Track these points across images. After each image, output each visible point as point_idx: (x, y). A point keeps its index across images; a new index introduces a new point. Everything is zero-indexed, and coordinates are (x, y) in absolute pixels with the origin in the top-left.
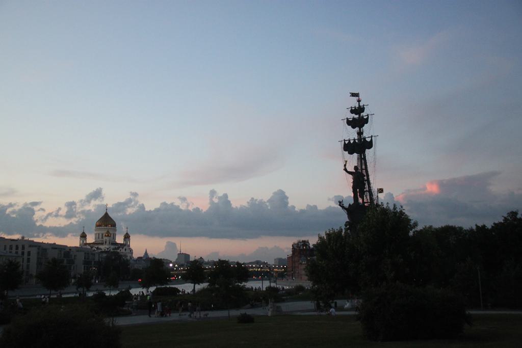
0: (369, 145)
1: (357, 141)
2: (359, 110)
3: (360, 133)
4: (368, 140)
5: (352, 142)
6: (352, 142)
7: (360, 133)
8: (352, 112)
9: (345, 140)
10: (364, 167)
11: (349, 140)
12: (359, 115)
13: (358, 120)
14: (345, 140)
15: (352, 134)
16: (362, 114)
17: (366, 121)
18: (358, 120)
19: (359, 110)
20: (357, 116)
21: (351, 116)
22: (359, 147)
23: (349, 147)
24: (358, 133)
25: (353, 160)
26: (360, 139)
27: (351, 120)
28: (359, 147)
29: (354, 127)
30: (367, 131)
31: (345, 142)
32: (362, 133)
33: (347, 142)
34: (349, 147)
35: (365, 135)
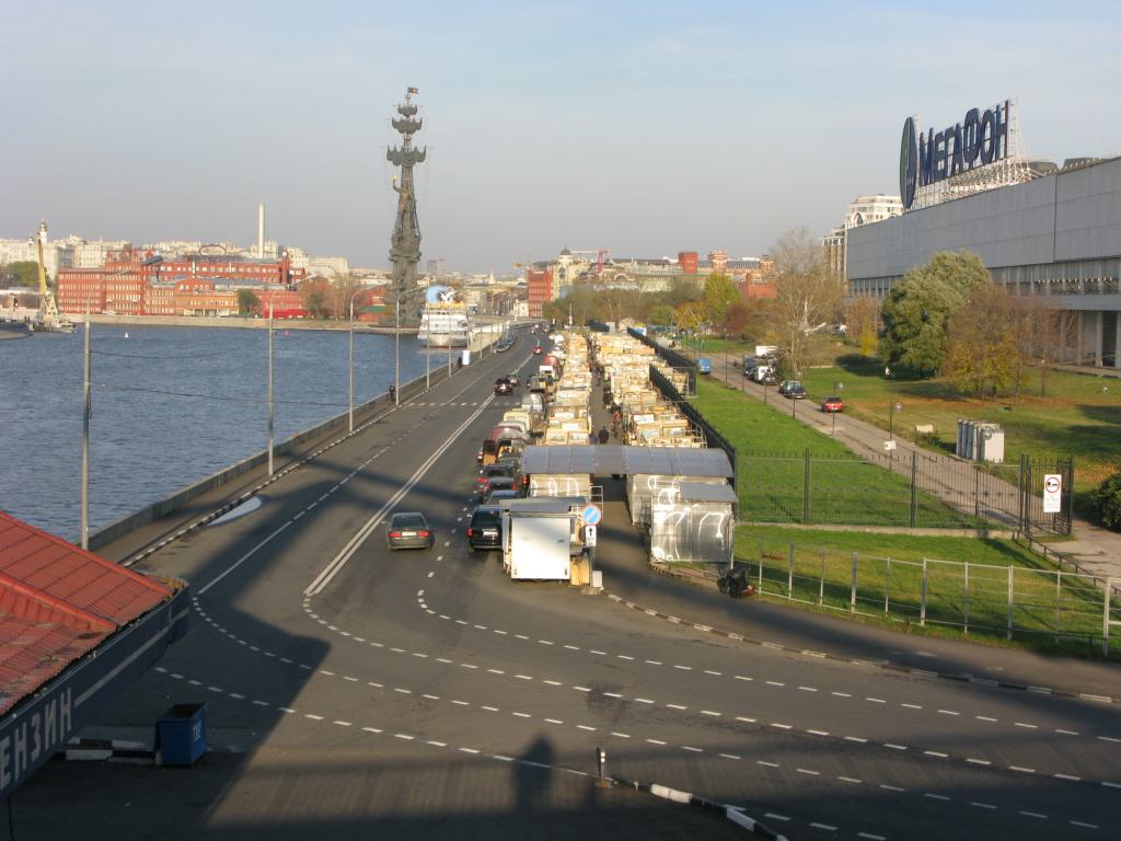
0: (422, 157)
3: (407, 141)
4: (421, 151)
5: (399, 150)
6: (399, 150)
7: (407, 141)
8: (400, 111)
13: (407, 126)
15: (396, 140)
17: (418, 126)
18: (407, 123)
19: (408, 111)
20: (404, 118)
21: (399, 117)
22: (406, 159)
23: (393, 156)
25: (396, 172)
28: (406, 159)
29: (401, 132)
30: (418, 141)
33: (392, 149)
34: (393, 156)
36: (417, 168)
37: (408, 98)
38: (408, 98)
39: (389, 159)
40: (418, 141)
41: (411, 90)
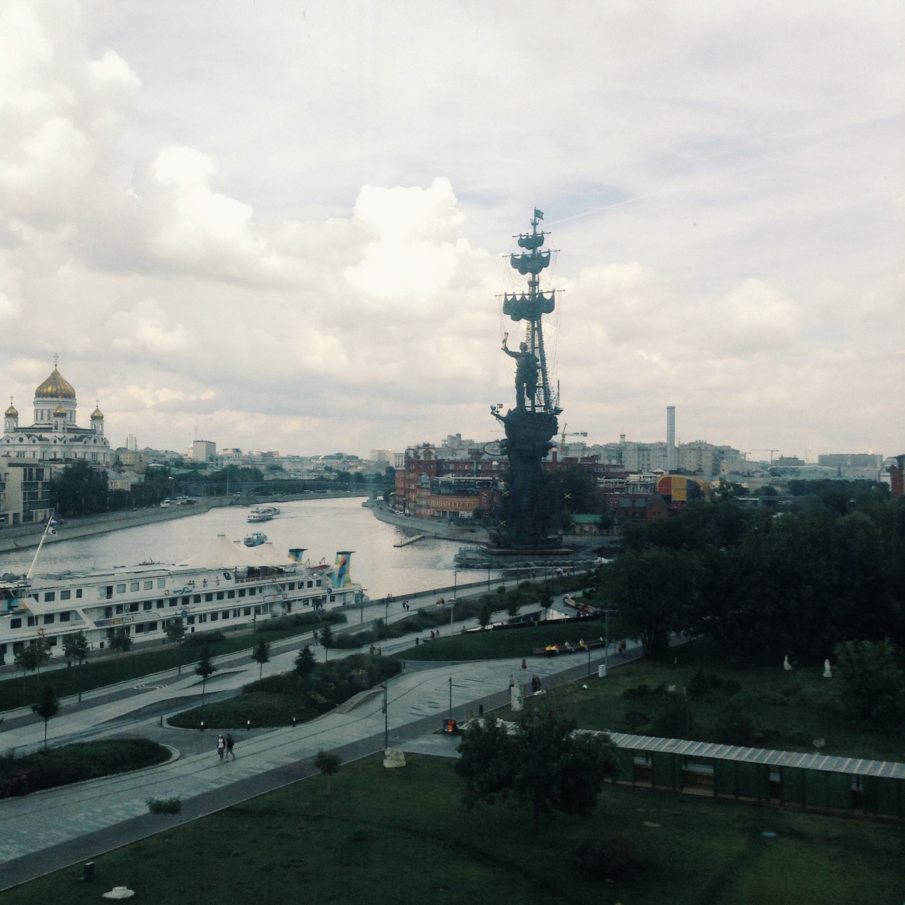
1: (527, 297)
2: (533, 242)
3: (534, 284)
5: (518, 298)
6: (518, 298)
7: (534, 284)
8: (523, 243)
9: (506, 295)
10: (537, 343)
11: (514, 295)
12: (534, 251)
13: (532, 260)
14: (506, 295)
16: (539, 248)
18: (532, 260)
19: (533, 242)
20: (530, 252)
21: (521, 251)
22: (531, 308)
24: (529, 283)
26: (533, 295)
27: (519, 257)
29: (523, 272)
30: (548, 281)
31: (506, 299)
32: (537, 283)
33: (509, 298)
35: (542, 287)
36: (547, 322)
37: (535, 224)
38: (535, 224)
39: (506, 312)
40: (548, 281)
41: (538, 214)
